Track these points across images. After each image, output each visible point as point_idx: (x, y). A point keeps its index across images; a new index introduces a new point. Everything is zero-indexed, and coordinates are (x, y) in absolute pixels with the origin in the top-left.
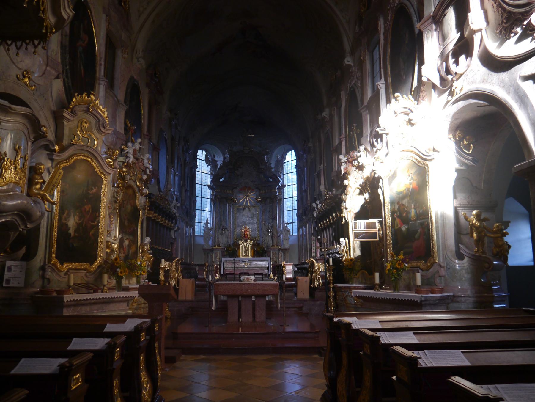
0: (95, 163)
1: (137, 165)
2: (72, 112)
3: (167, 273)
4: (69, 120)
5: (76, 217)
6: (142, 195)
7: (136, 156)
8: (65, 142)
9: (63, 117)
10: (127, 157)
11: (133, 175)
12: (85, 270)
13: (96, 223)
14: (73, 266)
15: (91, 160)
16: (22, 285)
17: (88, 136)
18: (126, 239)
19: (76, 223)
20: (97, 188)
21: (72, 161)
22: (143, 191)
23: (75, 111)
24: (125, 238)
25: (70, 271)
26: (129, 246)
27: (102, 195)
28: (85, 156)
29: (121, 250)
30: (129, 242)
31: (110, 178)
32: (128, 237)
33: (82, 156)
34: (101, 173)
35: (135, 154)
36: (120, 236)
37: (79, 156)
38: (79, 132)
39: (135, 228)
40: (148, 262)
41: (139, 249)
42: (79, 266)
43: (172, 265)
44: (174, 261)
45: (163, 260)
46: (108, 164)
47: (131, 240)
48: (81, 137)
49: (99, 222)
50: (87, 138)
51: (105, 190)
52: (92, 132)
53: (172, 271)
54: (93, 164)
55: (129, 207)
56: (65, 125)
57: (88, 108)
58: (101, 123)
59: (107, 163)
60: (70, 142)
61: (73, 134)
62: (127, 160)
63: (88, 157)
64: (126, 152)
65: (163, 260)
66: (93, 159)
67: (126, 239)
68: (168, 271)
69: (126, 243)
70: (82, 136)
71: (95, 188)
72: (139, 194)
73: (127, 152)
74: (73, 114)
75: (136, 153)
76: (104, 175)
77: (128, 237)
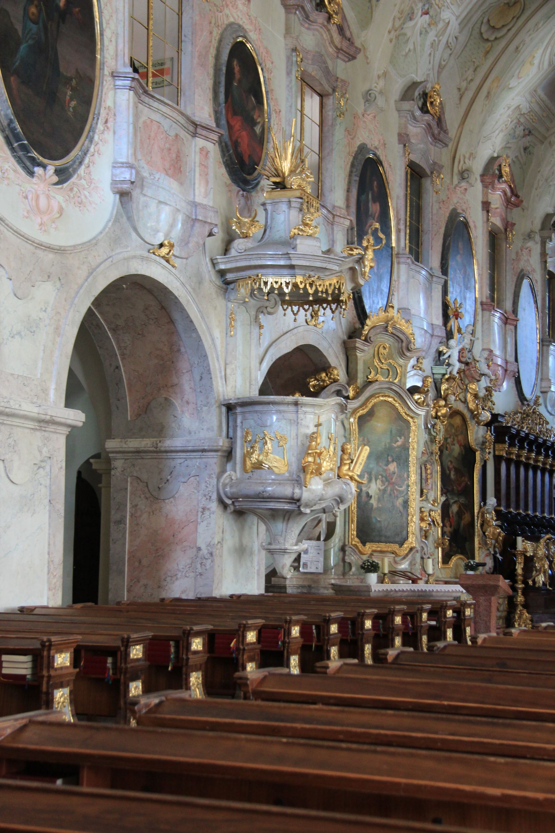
0: (399, 404)
1: (467, 372)
2: (366, 340)
3: (529, 561)
4: (363, 351)
5: (378, 481)
6: (478, 423)
7: (463, 360)
8: (360, 381)
9: (355, 348)
10: (449, 365)
11: (461, 391)
12: (393, 553)
13: (404, 487)
14: (377, 547)
15: (394, 400)
16: (322, 571)
17: (389, 366)
18: (455, 502)
19: (379, 489)
20: (403, 438)
21: (370, 405)
22: (480, 418)
23: (370, 338)
24: (452, 501)
25: (375, 554)
26: (460, 514)
27: (411, 447)
28: (385, 396)
29: (446, 521)
30: (460, 507)
31: (421, 421)
32: (456, 499)
33: (383, 396)
34: (408, 415)
35: (462, 357)
36: (443, 499)
37: (378, 397)
38: (376, 364)
39: (469, 483)
40: (493, 541)
41: (476, 518)
42: (385, 547)
43: (537, 547)
44: (542, 541)
45: (519, 539)
46: (416, 402)
47: (462, 504)
48: (379, 369)
49: (408, 486)
50: (388, 369)
51: (414, 439)
52: (393, 359)
53: (537, 558)
54: (397, 405)
55: (457, 449)
56: (359, 357)
57: (387, 327)
58: (404, 345)
59: (414, 400)
60: (366, 379)
61: (369, 368)
62: (449, 371)
63: (389, 397)
64: (446, 356)
65: (519, 539)
66: (396, 399)
67: (455, 502)
68: (532, 558)
69: (455, 508)
70: (381, 368)
71: (401, 438)
72: (474, 422)
73: (449, 356)
74: (368, 342)
75: (464, 355)
76: (412, 418)
77: (456, 499)
